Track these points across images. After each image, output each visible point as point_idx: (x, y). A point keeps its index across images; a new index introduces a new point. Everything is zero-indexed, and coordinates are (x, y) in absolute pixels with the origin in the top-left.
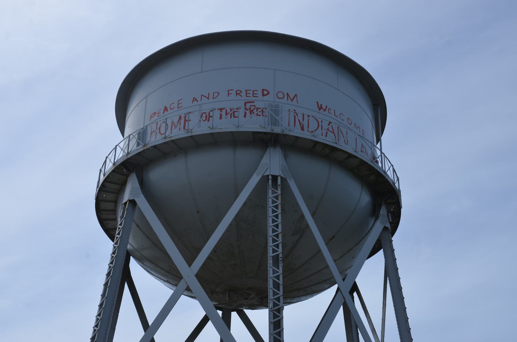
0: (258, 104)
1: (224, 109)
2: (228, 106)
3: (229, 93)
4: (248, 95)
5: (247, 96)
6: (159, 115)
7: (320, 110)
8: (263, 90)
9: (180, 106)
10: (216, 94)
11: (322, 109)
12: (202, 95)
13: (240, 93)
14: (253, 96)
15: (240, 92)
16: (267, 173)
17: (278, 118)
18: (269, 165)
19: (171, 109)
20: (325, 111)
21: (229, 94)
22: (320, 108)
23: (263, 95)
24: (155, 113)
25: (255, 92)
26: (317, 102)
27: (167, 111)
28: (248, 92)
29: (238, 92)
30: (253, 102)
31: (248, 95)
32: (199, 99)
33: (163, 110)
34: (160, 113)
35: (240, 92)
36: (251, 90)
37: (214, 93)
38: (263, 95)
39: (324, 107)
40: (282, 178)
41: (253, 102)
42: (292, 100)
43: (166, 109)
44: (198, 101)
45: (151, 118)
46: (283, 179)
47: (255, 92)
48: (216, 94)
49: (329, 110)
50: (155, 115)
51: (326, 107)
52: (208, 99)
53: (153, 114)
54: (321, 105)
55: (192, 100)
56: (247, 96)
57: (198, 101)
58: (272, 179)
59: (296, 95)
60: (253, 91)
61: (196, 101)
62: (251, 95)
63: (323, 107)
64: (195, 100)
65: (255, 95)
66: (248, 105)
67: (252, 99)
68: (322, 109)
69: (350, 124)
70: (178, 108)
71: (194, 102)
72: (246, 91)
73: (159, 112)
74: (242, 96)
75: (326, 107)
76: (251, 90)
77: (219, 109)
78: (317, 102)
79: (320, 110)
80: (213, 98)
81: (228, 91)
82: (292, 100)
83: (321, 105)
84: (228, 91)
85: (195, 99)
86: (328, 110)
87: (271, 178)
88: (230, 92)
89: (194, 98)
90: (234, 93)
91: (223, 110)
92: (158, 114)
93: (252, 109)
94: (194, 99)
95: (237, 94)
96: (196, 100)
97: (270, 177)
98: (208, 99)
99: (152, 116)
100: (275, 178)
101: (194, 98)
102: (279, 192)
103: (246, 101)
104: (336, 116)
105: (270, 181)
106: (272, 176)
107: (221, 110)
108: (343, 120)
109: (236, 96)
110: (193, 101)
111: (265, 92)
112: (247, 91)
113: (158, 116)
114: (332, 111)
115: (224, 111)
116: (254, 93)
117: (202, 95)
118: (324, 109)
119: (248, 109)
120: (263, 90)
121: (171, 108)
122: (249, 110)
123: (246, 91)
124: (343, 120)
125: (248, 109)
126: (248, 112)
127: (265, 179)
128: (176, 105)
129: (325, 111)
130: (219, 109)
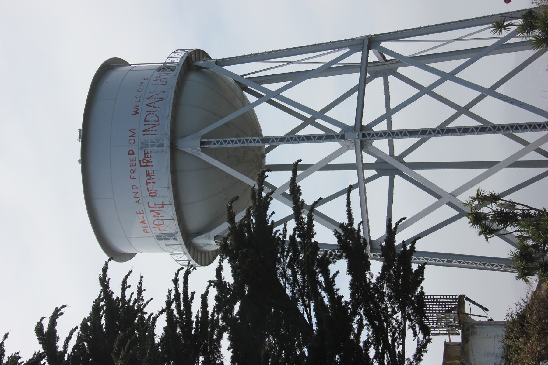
0: (142, 157)
1: (146, 181)
2: (145, 178)
3: (133, 178)
4: (134, 165)
5: (135, 166)
6: (146, 227)
7: (138, 113)
8: (129, 154)
9: (142, 212)
10: (134, 187)
11: (137, 111)
12: (135, 197)
13: (133, 170)
14: (135, 161)
15: (132, 171)
16: (199, 149)
17: (157, 144)
18: (192, 148)
19: (144, 218)
20: (138, 109)
21: (134, 178)
22: (136, 113)
23: (133, 154)
24: (144, 230)
25: (132, 160)
26: (132, 115)
27: (144, 221)
28: (132, 165)
29: (132, 172)
30: (140, 161)
31: (134, 165)
32: (138, 199)
33: (144, 225)
34: (145, 226)
35: (132, 171)
36: (130, 163)
37: (133, 189)
38: (133, 154)
39: (135, 110)
40: (202, 138)
41: (140, 161)
42: (135, 133)
43: (143, 222)
44: (139, 200)
45: (147, 232)
46: (203, 137)
47: (132, 160)
48: (134, 187)
49: (136, 106)
50: (145, 229)
51: (134, 108)
52: (137, 192)
53: (144, 231)
54: (134, 112)
55: (138, 204)
56: (135, 166)
57: (139, 200)
58: (203, 145)
59: (130, 131)
60: (130, 161)
61: (139, 201)
62: (134, 163)
63: (135, 111)
64: (138, 202)
65: (134, 160)
66: (143, 164)
67: (137, 162)
68: (137, 111)
69: (142, 90)
70: (143, 213)
71: (139, 202)
72: (131, 166)
73: (144, 227)
74: (135, 169)
75: (134, 108)
76: (130, 163)
77: (147, 185)
78: (132, 115)
79: (138, 113)
80: (138, 189)
81: (131, 179)
82: (135, 133)
83: (134, 112)
84: (131, 179)
85: (138, 202)
86: (137, 106)
87: (203, 146)
88: (132, 177)
89: (136, 203)
90: (132, 175)
91: (148, 182)
92: (145, 227)
93: (146, 161)
94: (138, 202)
95: (134, 172)
96: (138, 201)
97: (202, 146)
98: (137, 192)
99: (146, 231)
100: (202, 143)
101: (136, 203)
102: (213, 140)
103: (140, 166)
104: (140, 101)
105: (206, 146)
106: (201, 145)
107: (147, 183)
108: (141, 95)
109: (135, 173)
110: (139, 203)
111: (131, 152)
112: (131, 165)
113: (147, 227)
114: (137, 104)
115: (148, 181)
116: (132, 160)
117: (135, 197)
118: (137, 110)
119: (146, 164)
120: (129, 154)
121: (143, 218)
122: (147, 163)
123: (131, 166)
124: (141, 95)
125: (146, 164)
126: (148, 164)
127: (203, 150)
128: (140, 215)
129: (138, 109)
130: (147, 185)
